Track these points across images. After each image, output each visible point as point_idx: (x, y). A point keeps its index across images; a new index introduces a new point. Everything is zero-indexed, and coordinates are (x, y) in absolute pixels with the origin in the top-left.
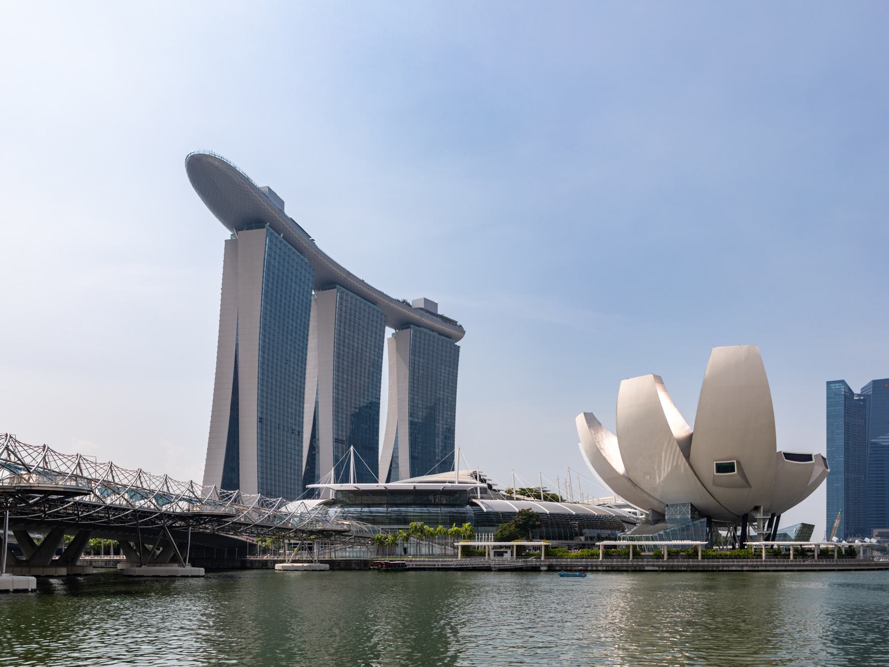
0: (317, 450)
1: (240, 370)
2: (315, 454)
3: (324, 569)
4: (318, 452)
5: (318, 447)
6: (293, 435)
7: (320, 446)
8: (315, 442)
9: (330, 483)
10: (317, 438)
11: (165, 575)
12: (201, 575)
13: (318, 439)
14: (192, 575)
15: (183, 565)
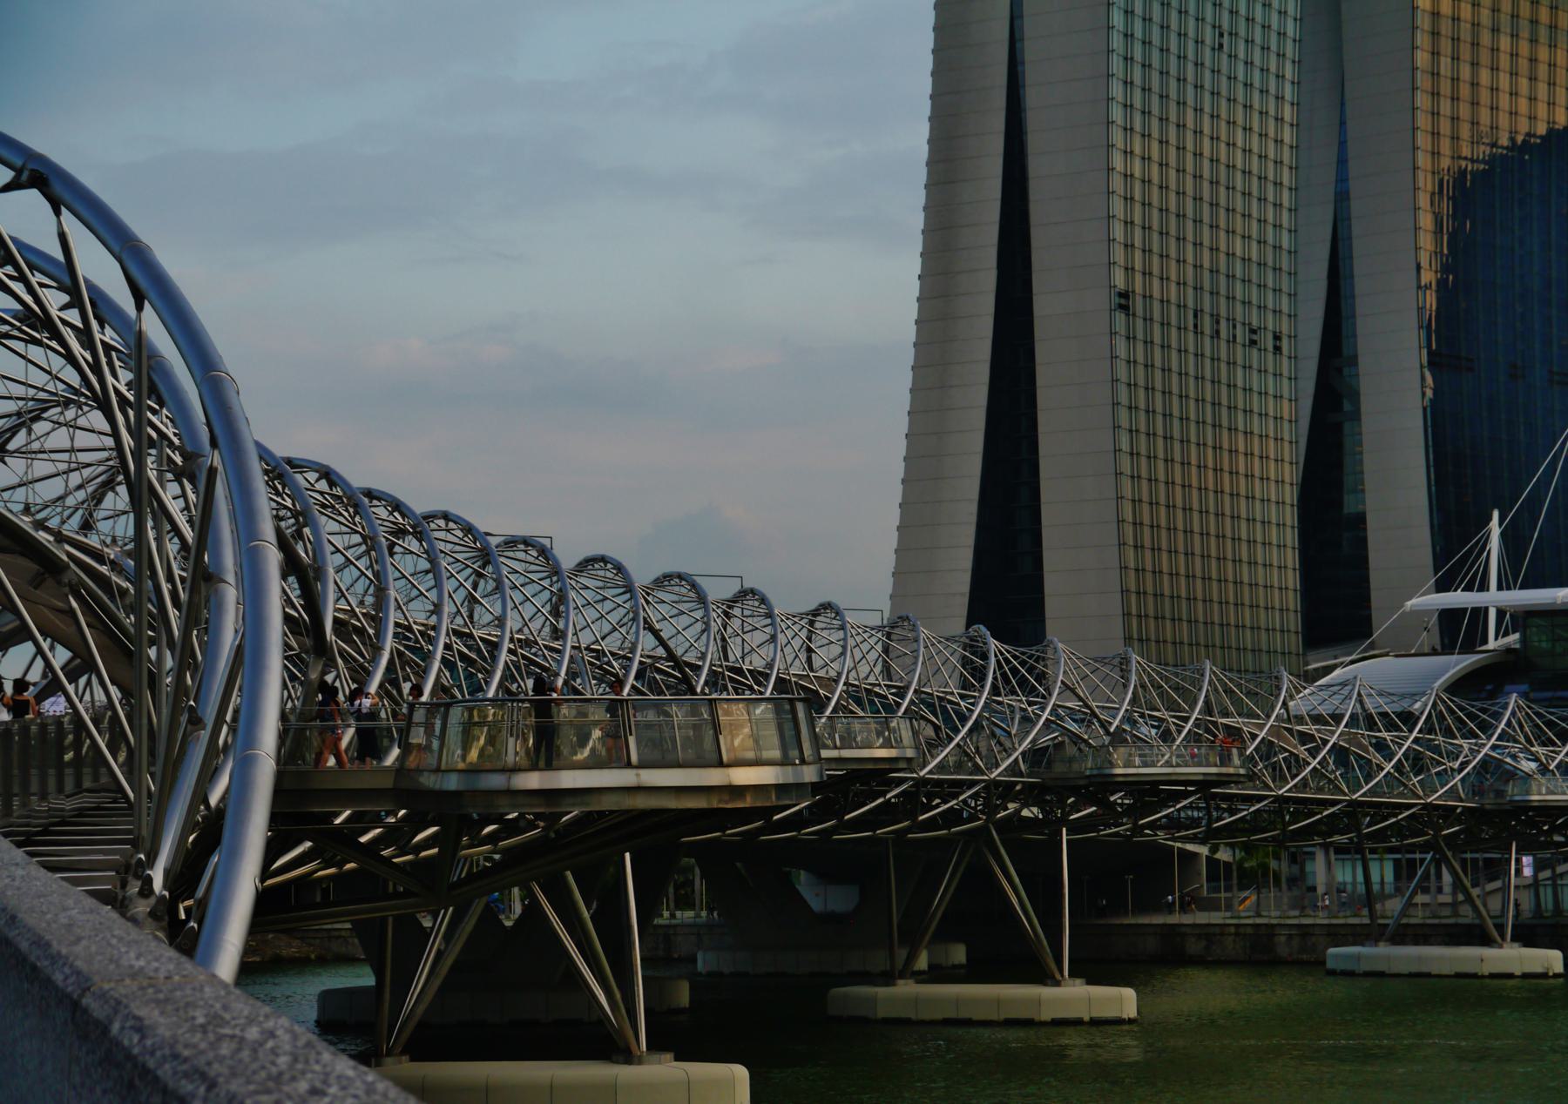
0: (1347, 406)
1: (1033, 98)
2: (1338, 428)
3: (1539, 970)
4: (1356, 416)
5: (1355, 396)
6: (1255, 352)
7: (1362, 392)
8: (1340, 370)
9: (1484, 587)
10: (1346, 351)
11: (994, 1017)
12: (1125, 1016)
13: (1353, 361)
14: (1095, 1015)
15: (1053, 977)
